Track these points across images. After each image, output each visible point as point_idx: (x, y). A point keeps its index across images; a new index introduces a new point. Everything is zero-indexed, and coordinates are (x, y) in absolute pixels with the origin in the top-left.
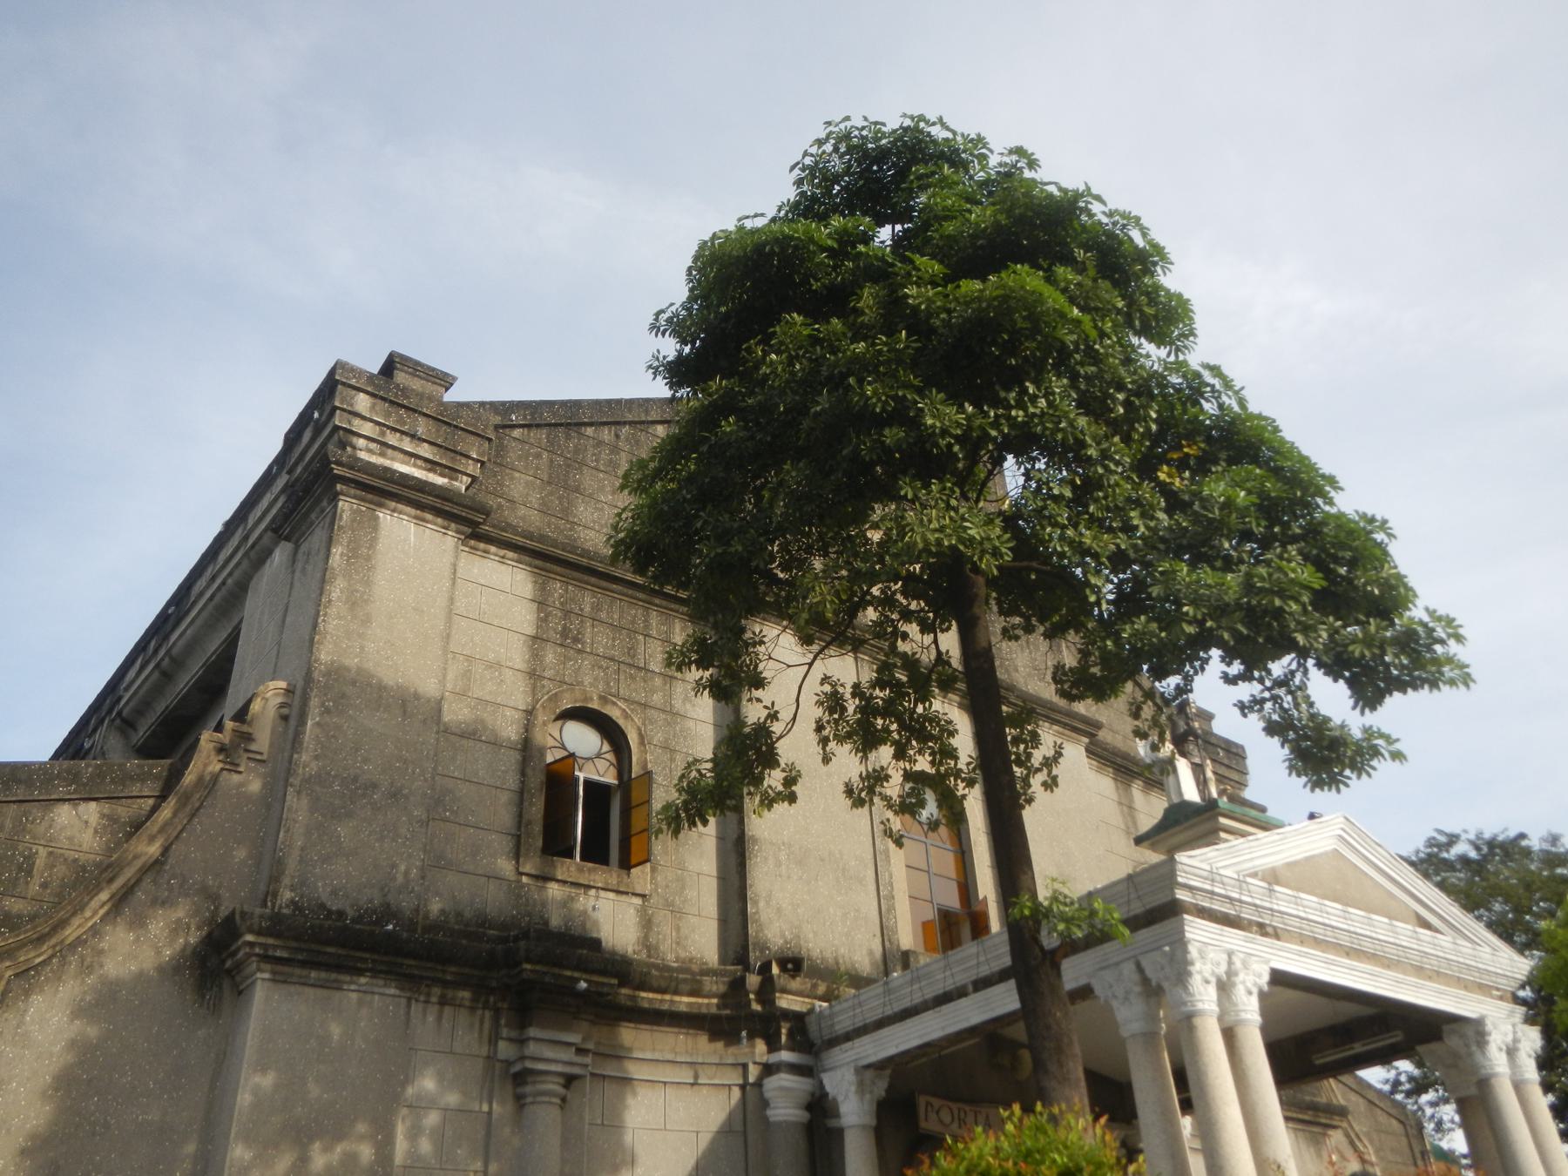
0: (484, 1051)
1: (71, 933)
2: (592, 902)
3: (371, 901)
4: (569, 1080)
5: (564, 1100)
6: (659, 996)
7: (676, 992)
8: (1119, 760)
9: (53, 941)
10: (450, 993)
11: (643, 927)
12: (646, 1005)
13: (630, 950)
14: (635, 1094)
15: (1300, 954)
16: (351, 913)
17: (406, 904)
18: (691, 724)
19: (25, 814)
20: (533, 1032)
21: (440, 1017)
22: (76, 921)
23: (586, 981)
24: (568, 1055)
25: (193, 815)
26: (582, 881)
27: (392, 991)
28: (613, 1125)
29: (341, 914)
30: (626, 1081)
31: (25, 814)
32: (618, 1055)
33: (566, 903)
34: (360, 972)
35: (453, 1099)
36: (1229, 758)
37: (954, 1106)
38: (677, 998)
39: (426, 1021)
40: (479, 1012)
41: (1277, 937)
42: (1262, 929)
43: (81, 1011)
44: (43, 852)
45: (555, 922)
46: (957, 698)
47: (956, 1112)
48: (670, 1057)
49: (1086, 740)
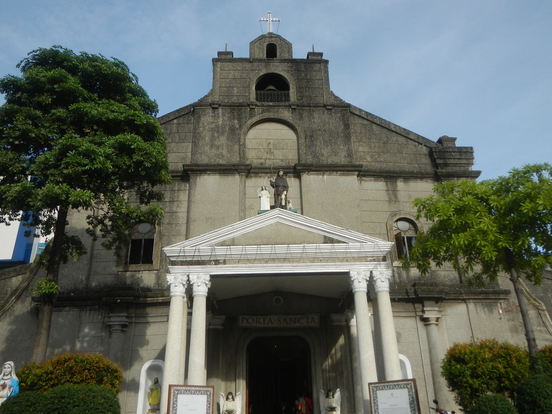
0: (102, 320)
1: (6, 307)
2: (141, 275)
3: (71, 288)
4: (124, 326)
5: (122, 330)
6: (153, 299)
7: (157, 297)
8: (385, 174)
9: (3, 310)
10: (92, 307)
11: (157, 279)
12: (149, 302)
13: (152, 286)
14: (150, 326)
15: (232, 267)
16: (65, 291)
17: (81, 287)
18: (179, 214)
19: (6, 281)
20: (111, 315)
21: (90, 314)
22: (7, 305)
23: (120, 299)
24: (124, 319)
25: (34, 275)
26: (137, 270)
27: (76, 310)
28: (143, 335)
29: (63, 293)
30: (148, 323)
31: (6, 281)
32: (145, 316)
33: (133, 276)
34: (66, 307)
35: (93, 332)
36: (460, 155)
37: (254, 318)
38: (158, 298)
39: (86, 316)
40: (101, 311)
41: (225, 262)
42: (217, 262)
43: (11, 323)
44: (9, 289)
45: (128, 281)
46: (292, 175)
47: (255, 319)
48: (159, 314)
49: (357, 173)
